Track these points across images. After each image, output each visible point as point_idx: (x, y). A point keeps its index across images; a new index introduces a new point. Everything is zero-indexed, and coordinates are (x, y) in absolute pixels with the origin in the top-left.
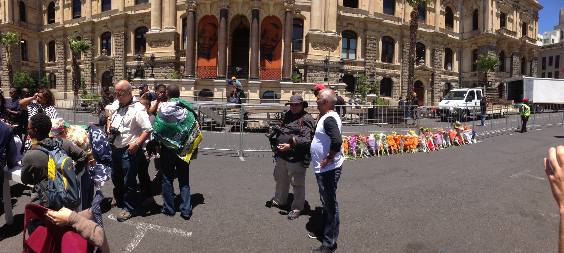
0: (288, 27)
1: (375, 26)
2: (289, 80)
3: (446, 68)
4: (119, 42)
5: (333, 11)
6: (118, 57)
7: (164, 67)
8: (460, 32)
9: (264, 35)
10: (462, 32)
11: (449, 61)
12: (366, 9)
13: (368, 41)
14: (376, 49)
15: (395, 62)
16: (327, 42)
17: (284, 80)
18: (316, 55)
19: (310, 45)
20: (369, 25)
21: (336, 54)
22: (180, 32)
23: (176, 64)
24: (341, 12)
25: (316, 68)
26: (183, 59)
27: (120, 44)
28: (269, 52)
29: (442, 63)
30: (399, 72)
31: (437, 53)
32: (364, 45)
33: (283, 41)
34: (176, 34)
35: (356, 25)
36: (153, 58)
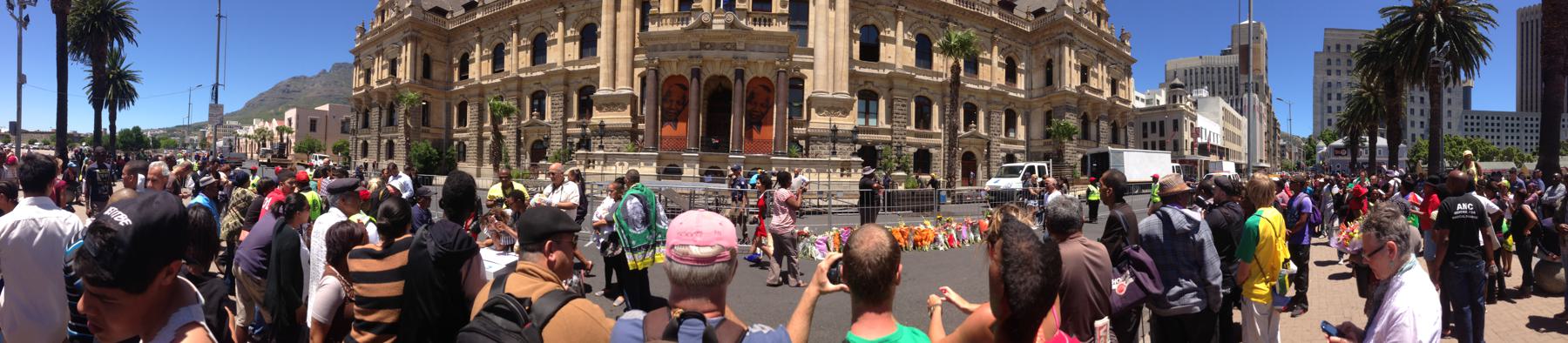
0: (782, 90)
1: (905, 83)
2: (783, 154)
5: (843, 66)
9: (750, 98)
12: (892, 61)
17: (776, 154)
18: (819, 122)
20: (896, 82)
22: (638, 93)
23: (633, 134)
24: (857, 68)
25: (821, 138)
26: (641, 126)
28: (757, 118)
30: (941, 141)
32: (890, 107)
34: (633, 97)
35: (877, 83)
36: (602, 125)
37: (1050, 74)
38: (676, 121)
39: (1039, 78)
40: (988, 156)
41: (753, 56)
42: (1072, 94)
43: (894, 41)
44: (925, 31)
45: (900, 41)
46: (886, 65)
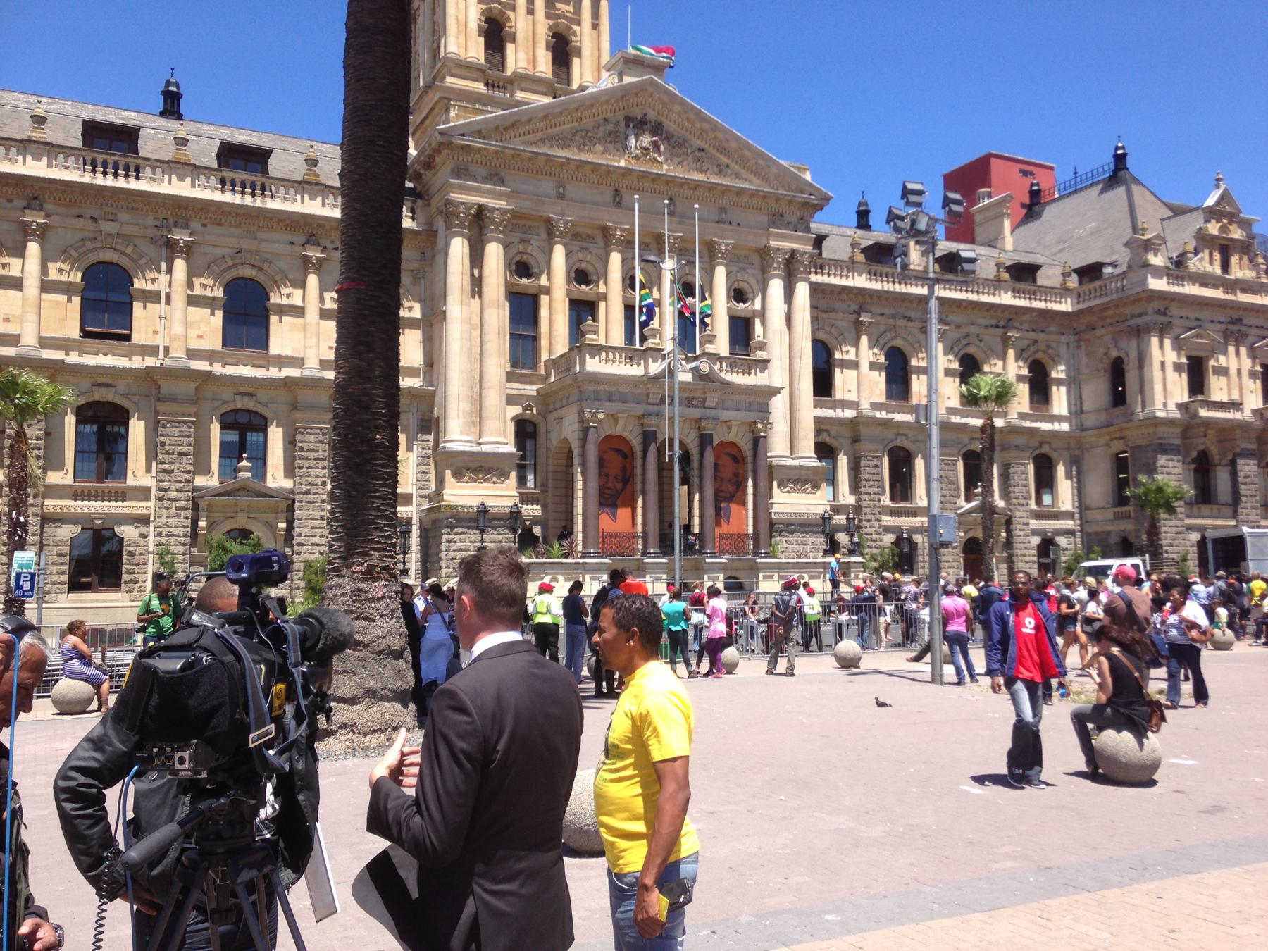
1: (876, 431)
3: (1039, 502)
4: (312, 451)
6: (307, 492)
7: (494, 528)
8: (1070, 412)
10: (1077, 410)
11: (1045, 481)
13: (863, 463)
14: (879, 477)
15: (918, 500)
19: (775, 483)
20: (864, 431)
21: (821, 498)
29: (1028, 492)
31: (1016, 471)
32: (855, 469)
33: (750, 483)
37: (1120, 382)
38: (614, 506)
39: (1097, 391)
40: (1009, 544)
42: (1170, 422)
43: (855, 365)
44: (898, 343)
45: (865, 365)
46: (845, 404)
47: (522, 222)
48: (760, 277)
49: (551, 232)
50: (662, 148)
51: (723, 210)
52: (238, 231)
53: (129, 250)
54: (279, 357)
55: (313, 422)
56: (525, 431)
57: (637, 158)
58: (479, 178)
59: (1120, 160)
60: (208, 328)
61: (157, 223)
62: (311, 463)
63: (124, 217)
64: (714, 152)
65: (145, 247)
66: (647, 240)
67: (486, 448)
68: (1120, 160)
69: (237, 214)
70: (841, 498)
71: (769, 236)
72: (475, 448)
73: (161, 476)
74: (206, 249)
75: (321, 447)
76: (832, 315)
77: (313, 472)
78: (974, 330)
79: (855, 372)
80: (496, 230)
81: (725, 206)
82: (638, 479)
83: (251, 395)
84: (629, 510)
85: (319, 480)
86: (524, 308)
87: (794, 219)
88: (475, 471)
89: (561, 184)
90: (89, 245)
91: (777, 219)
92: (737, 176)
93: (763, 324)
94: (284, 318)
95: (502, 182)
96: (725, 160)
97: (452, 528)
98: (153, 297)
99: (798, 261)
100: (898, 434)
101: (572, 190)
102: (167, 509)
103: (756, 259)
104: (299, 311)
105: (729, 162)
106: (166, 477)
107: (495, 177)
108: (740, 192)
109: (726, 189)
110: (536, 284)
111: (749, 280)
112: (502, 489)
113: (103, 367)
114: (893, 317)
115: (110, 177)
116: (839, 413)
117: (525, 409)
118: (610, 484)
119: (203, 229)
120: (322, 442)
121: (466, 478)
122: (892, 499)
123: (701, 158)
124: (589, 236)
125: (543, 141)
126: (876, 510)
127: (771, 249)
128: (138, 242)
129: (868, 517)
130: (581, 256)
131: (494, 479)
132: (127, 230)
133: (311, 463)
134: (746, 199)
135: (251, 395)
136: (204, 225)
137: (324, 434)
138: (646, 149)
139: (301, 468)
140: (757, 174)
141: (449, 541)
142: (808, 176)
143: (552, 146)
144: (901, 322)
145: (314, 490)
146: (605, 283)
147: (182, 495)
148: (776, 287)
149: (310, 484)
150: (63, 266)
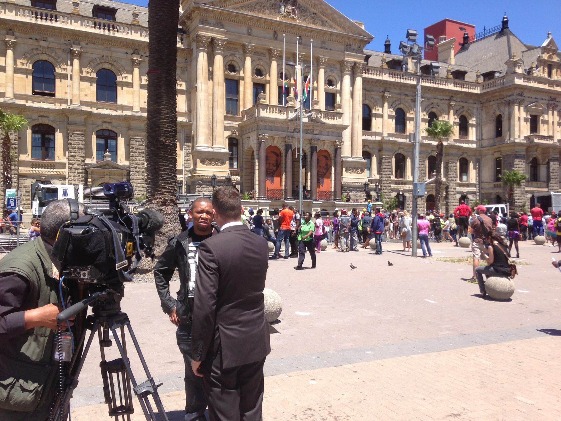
1: (390, 146)
3: (461, 179)
4: (137, 149)
6: (136, 168)
8: (477, 139)
10: (480, 139)
11: (464, 170)
13: (383, 161)
14: (390, 167)
15: (407, 178)
16: (357, 167)
19: (344, 169)
20: (384, 146)
27: (138, 151)
29: (456, 175)
31: (451, 165)
32: (380, 163)
33: (333, 169)
37: (500, 126)
38: (273, 176)
39: (489, 130)
40: (446, 198)
41: (323, 138)
42: (521, 144)
43: (381, 116)
44: (401, 106)
45: (386, 116)
46: (376, 134)
47: (232, 46)
48: (340, 74)
49: (245, 51)
50: (296, 12)
51: (323, 42)
52: (102, 47)
53: (53, 55)
54: (122, 106)
55: (138, 136)
56: (233, 143)
57: (285, 16)
58: (212, 25)
59: (505, 24)
60: (89, 91)
61: (66, 42)
62: (137, 154)
63: (50, 39)
64: (320, 15)
65: (60, 53)
66: (289, 56)
67: (215, 150)
68: (505, 24)
69: (102, 39)
70: (373, 176)
71: (344, 55)
72: (211, 150)
73: (70, 158)
74: (88, 55)
75: (141, 147)
76: (372, 93)
77: (138, 158)
78: (436, 101)
79: (381, 119)
80: (220, 49)
81: (325, 39)
82: (283, 166)
83: (110, 123)
84: (279, 179)
85: (141, 162)
86: (233, 86)
87: (356, 47)
88: (211, 160)
89: (250, 28)
90: (35, 52)
91: (349, 47)
92: (331, 26)
93: (341, 96)
94: (124, 88)
95: (223, 27)
96: (325, 19)
97: (201, 185)
98: (65, 77)
99: (357, 67)
100: (399, 148)
101: (255, 31)
102: (74, 173)
103: (338, 66)
104: (130, 85)
105: (327, 19)
106: (73, 158)
107: (219, 24)
108: (332, 34)
109: (325, 33)
110: (238, 75)
111: (334, 75)
112: (222, 169)
113: (43, 108)
114: (400, 94)
115: (44, 20)
116: (373, 138)
117: (233, 133)
118: (271, 168)
119: (87, 46)
120: (142, 145)
121: (207, 163)
122: (396, 177)
123: (314, 17)
124: (262, 53)
125: (241, 7)
126: (389, 182)
127: (345, 61)
128: (57, 51)
129: (385, 185)
130: (258, 62)
131: (219, 164)
132: (52, 45)
133: (137, 154)
134: (334, 37)
135: (110, 123)
136: (87, 44)
137: (143, 142)
138: (289, 12)
139: (133, 156)
140: (339, 25)
141: (199, 191)
142: (363, 27)
143: (246, 10)
144: (403, 97)
145: (139, 166)
146: (269, 75)
147: (80, 167)
148: (347, 79)
149: (137, 164)
150: (23, 61)
